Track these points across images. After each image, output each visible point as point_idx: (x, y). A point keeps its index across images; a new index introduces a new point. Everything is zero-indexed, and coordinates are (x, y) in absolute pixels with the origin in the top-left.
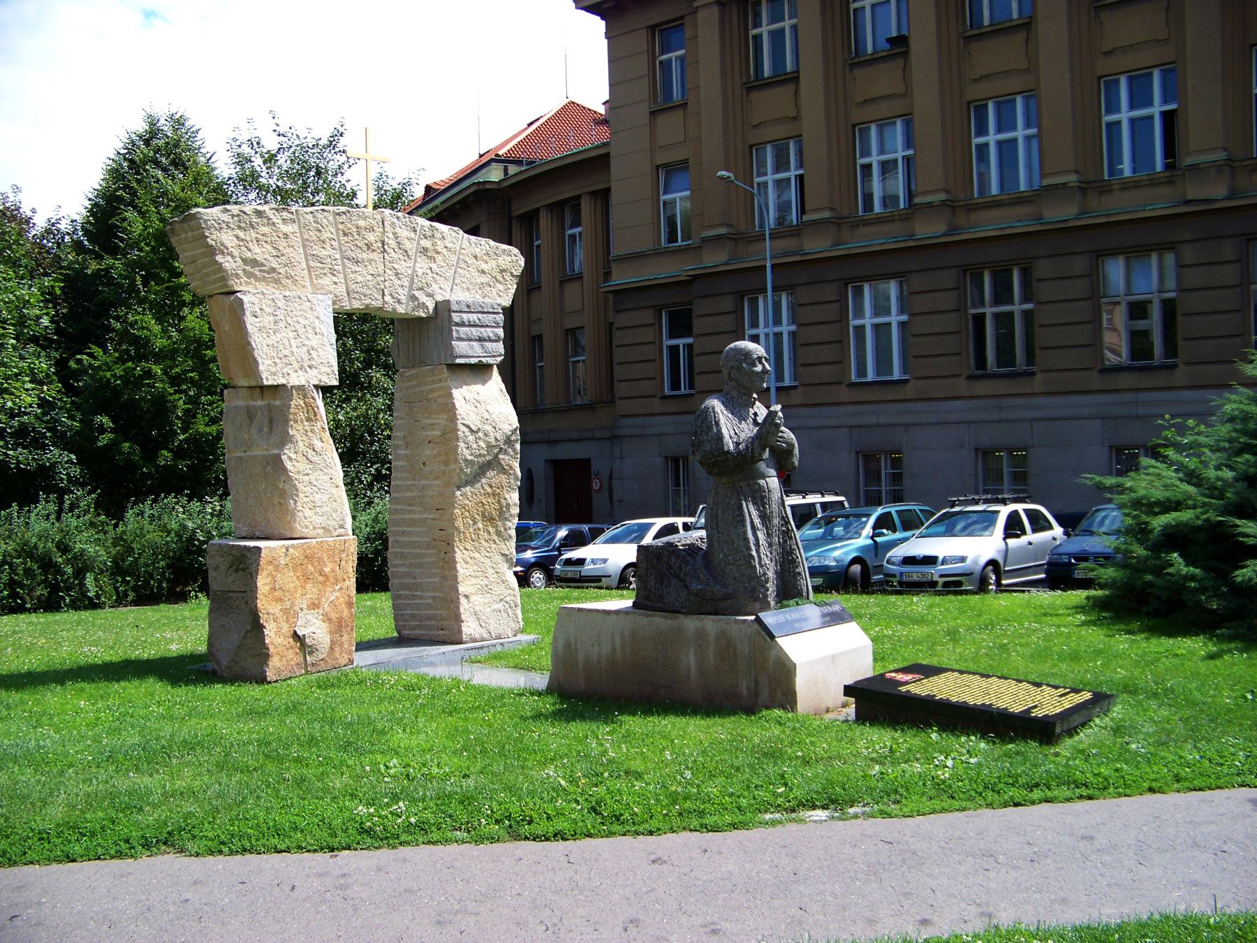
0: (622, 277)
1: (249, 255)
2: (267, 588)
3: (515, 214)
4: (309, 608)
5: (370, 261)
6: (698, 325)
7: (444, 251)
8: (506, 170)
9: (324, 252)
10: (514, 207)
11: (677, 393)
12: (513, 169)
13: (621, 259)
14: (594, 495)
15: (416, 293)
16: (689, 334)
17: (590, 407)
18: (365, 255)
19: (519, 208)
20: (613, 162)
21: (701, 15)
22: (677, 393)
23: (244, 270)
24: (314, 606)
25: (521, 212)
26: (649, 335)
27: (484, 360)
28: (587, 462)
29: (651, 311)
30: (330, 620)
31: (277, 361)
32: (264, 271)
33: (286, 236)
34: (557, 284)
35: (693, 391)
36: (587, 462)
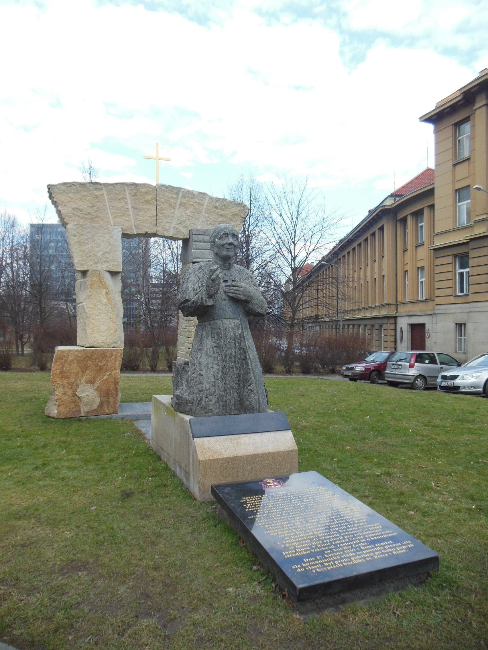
0: (439, 242)
1: (76, 206)
2: (58, 371)
3: (399, 218)
4: (87, 383)
5: (148, 210)
6: (472, 262)
7: (195, 204)
8: (395, 200)
10: (398, 215)
11: (462, 294)
12: (397, 199)
13: (438, 234)
14: (426, 339)
15: (177, 226)
16: (468, 267)
17: (426, 301)
18: (145, 207)
19: (400, 216)
20: (436, 191)
21: (478, 112)
22: (462, 294)
23: (73, 214)
24: (91, 382)
25: (400, 217)
26: (450, 268)
28: (423, 325)
29: (451, 257)
32: (84, 214)
33: (97, 197)
34: (414, 248)
35: (469, 293)
36: (423, 325)
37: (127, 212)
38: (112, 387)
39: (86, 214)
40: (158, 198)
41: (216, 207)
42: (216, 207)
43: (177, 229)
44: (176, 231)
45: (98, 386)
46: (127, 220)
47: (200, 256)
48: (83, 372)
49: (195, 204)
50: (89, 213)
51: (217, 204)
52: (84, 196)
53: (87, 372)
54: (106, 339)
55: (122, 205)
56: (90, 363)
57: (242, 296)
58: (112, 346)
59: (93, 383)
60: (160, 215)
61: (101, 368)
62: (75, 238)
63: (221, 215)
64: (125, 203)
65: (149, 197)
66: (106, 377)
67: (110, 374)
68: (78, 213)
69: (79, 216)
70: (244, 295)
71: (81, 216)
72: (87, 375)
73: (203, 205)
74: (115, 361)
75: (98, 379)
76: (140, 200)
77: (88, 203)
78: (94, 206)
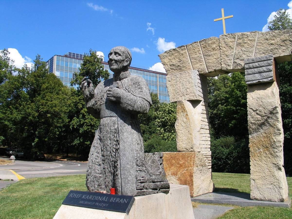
4: (172, 174)
5: (215, 54)
7: (249, 42)
9: (196, 56)
15: (236, 61)
18: (212, 53)
23: (171, 68)
27: (261, 80)
30: (181, 180)
31: (175, 94)
32: (176, 67)
33: (182, 54)
37: (201, 60)
38: (189, 179)
39: (177, 67)
40: (221, 45)
41: (267, 39)
42: (267, 39)
43: (236, 63)
44: (236, 64)
45: (179, 178)
46: (201, 65)
47: (251, 79)
48: (170, 167)
49: (249, 42)
50: (179, 66)
51: (267, 37)
52: (175, 56)
53: (172, 168)
54: (187, 145)
55: (198, 56)
56: (174, 161)
57: (112, 98)
58: (190, 150)
59: (176, 175)
60: (223, 56)
61: (181, 166)
62: (170, 82)
63: (271, 44)
64: (200, 54)
65: (214, 46)
66: (184, 171)
67: (187, 170)
68: (174, 68)
69: (174, 69)
70: (114, 97)
71: (175, 68)
72: (172, 169)
73: (254, 40)
74: (191, 161)
75: (179, 173)
76: (208, 49)
77: (177, 59)
78: (181, 61)
